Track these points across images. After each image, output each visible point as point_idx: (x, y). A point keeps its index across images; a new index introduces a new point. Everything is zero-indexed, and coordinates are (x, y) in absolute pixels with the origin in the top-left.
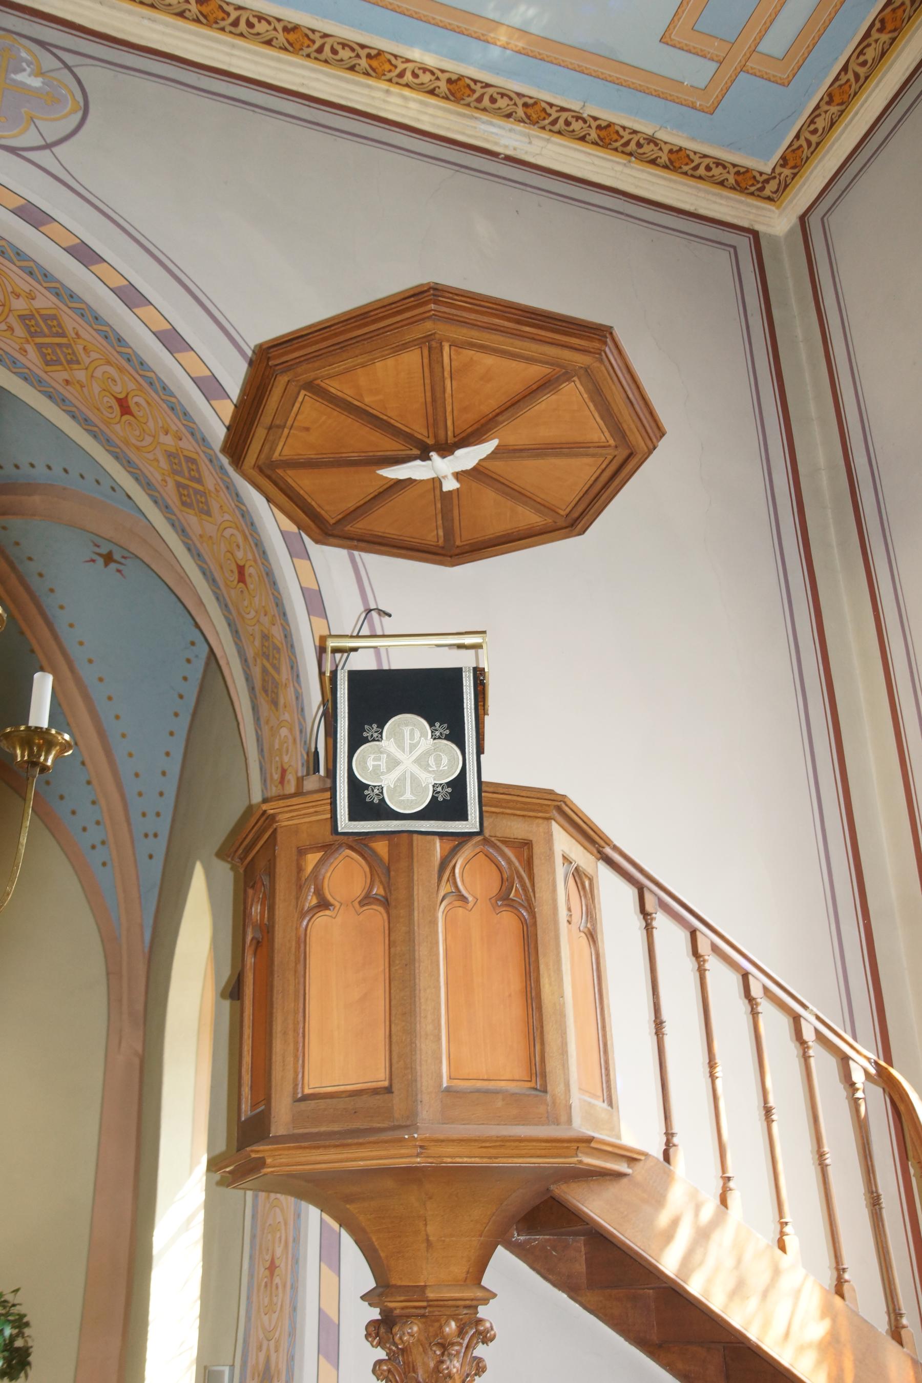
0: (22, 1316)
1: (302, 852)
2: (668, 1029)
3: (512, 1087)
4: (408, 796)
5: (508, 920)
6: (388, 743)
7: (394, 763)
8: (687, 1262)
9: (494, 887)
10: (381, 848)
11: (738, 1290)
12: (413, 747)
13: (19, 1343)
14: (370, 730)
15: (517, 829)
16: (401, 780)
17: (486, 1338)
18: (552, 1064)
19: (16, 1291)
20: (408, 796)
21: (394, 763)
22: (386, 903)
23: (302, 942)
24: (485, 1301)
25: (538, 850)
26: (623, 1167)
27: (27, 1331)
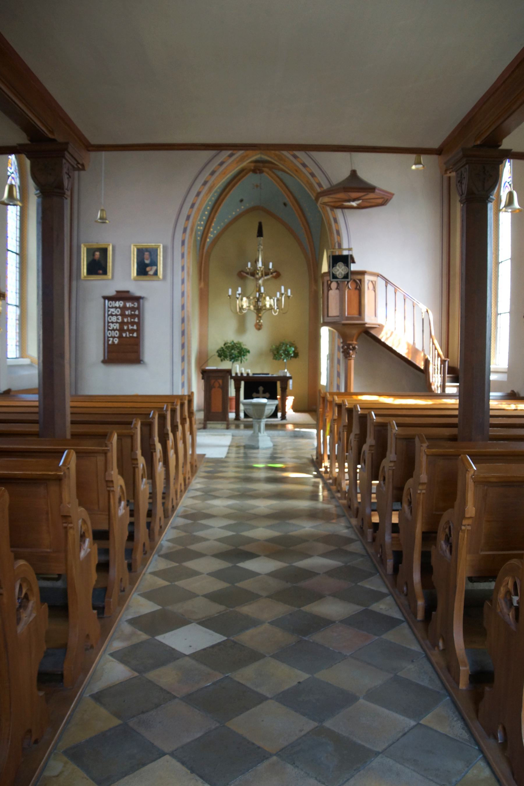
6: (338, 267)
8: (387, 339)
10: (339, 282)
12: (341, 267)
15: (359, 277)
16: (339, 273)
20: (340, 275)
25: (362, 280)
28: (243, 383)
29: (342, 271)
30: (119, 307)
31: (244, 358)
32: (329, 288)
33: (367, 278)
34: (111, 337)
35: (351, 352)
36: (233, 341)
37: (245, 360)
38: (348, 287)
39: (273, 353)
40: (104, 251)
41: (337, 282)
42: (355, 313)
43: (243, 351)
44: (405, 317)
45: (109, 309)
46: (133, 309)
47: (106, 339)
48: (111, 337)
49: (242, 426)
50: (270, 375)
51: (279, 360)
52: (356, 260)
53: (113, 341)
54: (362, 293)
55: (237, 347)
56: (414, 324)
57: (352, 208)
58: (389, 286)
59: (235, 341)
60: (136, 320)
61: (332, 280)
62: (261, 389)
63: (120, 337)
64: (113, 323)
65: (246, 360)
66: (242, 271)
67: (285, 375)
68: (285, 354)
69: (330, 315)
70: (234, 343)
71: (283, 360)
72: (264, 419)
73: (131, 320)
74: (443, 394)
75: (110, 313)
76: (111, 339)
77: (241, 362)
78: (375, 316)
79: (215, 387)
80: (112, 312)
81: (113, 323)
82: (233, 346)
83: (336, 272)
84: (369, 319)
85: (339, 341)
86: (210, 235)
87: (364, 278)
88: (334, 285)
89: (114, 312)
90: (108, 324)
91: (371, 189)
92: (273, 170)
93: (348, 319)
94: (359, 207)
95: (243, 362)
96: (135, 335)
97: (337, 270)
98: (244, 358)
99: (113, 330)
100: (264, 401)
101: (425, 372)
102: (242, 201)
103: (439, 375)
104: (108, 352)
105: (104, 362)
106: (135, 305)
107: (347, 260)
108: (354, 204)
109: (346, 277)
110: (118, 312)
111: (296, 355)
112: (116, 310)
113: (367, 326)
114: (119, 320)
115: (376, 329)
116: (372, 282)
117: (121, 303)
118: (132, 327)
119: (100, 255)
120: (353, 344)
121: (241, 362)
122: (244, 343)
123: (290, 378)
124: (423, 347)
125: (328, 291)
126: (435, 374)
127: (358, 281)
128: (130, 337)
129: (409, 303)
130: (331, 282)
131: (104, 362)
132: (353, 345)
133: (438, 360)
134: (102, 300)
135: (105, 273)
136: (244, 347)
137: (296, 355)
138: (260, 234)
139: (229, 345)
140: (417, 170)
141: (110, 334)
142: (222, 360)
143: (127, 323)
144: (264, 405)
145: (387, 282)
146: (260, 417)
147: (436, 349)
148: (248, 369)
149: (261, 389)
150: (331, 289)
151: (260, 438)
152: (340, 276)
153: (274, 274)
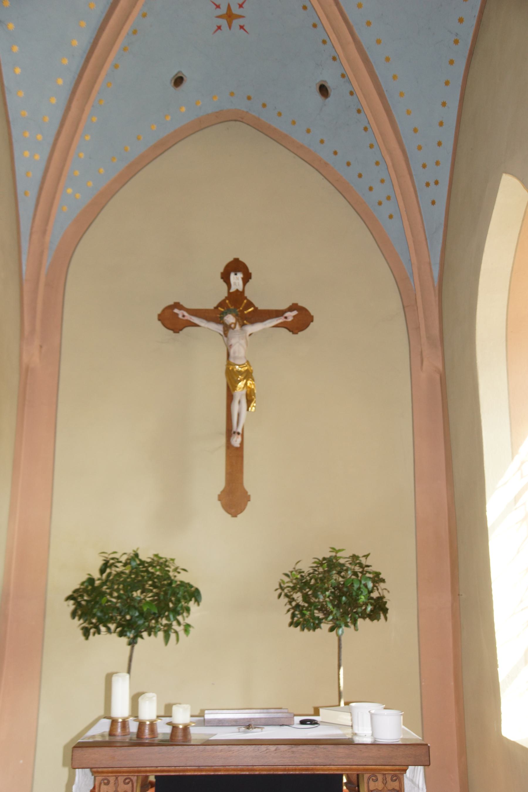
19: (366, 556)
27: (382, 585)
31: (179, 624)
36: (136, 555)
37: (180, 629)
39: (291, 600)
43: (174, 594)
55: (152, 576)
59: (145, 556)
65: (187, 628)
66: (177, 305)
68: (338, 606)
70: (142, 563)
77: (167, 638)
82: (135, 571)
95: (173, 636)
98: (179, 624)
102: (179, 81)
121: (167, 638)
122: (179, 563)
136: (182, 577)
139: (120, 568)
153: (290, 315)
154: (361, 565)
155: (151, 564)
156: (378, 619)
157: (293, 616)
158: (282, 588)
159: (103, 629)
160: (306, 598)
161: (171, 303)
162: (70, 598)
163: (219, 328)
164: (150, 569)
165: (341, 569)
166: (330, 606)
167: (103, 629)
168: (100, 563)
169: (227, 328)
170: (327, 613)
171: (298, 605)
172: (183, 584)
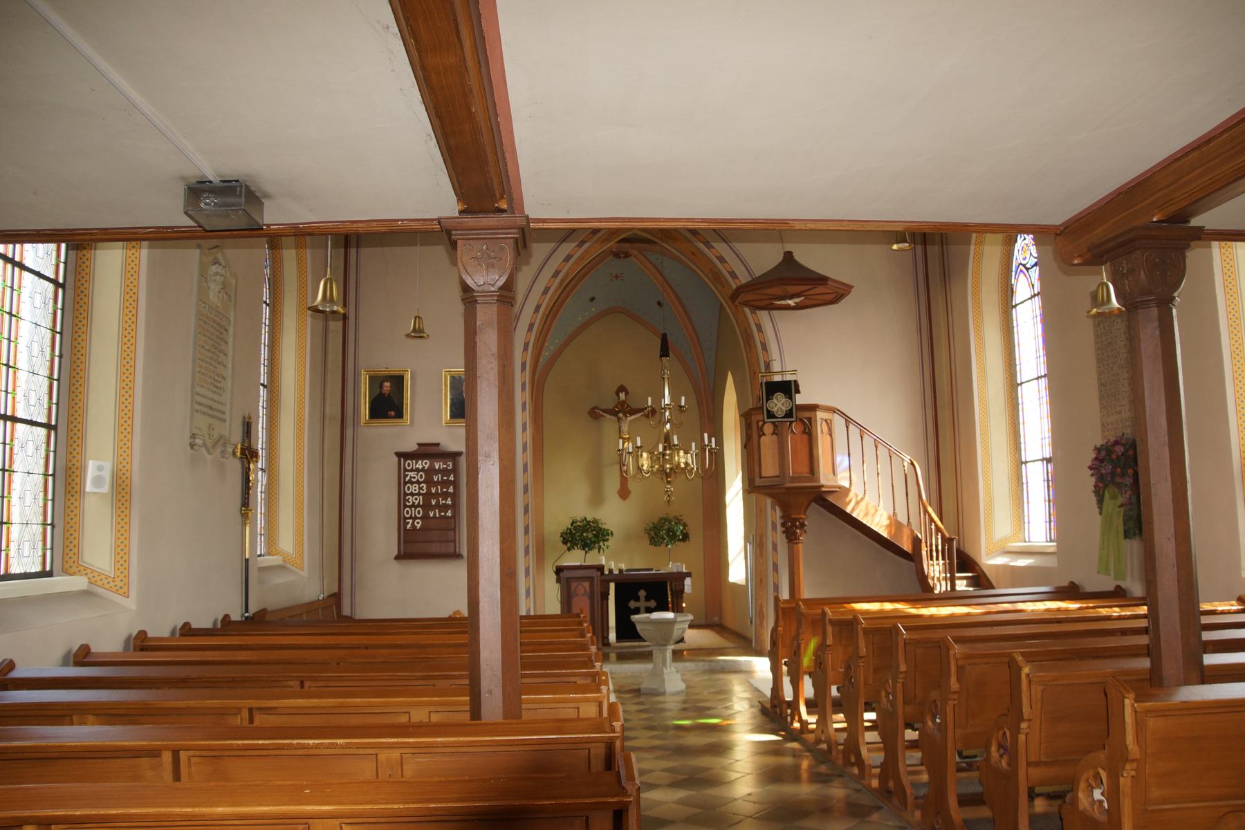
0: (685, 523)
1: (758, 422)
2: (851, 456)
3: (807, 475)
4: (780, 413)
5: (806, 436)
6: (775, 401)
7: (776, 405)
8: (853, 510)
9: (802, 428)
11: (866, 514)
13: (684, 531)
14: (770, 397)
15: (807, 414)
16: (778, 409)
17: (805, 525)
18: (816, 470)
20: (780, 413)
21: (776, 405)
22: (776, 434)
23: (759, 442)
24: (806, 518)
25: (813, 420)
26: (838, 490)
28: (612, 586)
29: (782, 407)
30: (423, 470)
31: (604, 545)
32: (761, 433)
33: (820, 415)
34: (410, 518)
35: (798, 531)
36: (585, 519)
37: (605, 548)
38: (792, 431)
39: (649, 535)
40: (398, 380)
41: (773, 423)
42: (804, 469)
44: (878, 474)
45: (407, 473)
46: (445, 472)
47: (402, 520)
48: (410, 518)
49: (613, 656)
50: (654, 572)
51: (660, 545)
52: (801, 389)
53: (413, 523)
54: (814, 440)
56: (892, 484)
57: (788, 308)
58: (851, 427)
60: (451, 490)
61: (766, 420)
62: (642, 593)
63: (425, 517)
64: (412, 495)
65: (608, 547)
66: (596, 407)
67: (680, 570)
68: (669, 536)
69: (763, 475)
71: (667, 545)
72: (670, 645)
73: (441, 490)
74: (954, 594)
75: (408, 479)
76: (411, 521)
77: (599, 551)
78: (834, 474)
79: (577, 595)
80: (411, 477)
81: (412, 495)
82: (585, 526)
83: (772, 408)
84: (825, 479)
85: (774, 515)
86: (543, 352)
87: (816, 416)
88: (768, 428)
89: (414, 478)
90: (405, 497)
91: (823, 280)
92: (645, 253)
93: (793, 479)
94: (798, 307)
95: (601, 550)
96: (449, 514)
97: (774, 405)
98: (604, 545)
99: (413, 506)
100: (670, 615)
101: (913, 557)
102: (592, 299)
103: (941, 562)
104: (405, 542)
105: (398, 558)
106: (448, 466)
107: (789, 388)
108: (791, 302)
109: (789, 414)
110: (421, 477)
111: (686, 537)
112: (417, 475)
113: (823, 489)
114: (423, 490)
115: (835, 494)
116: (826, 421)
117: (426, 463)
118: (444, 502)
119: (390, 387)
120: (801, 518)
121: (599, 551)
122: (603, 521)
123: (689, 575)
124: (909, 519)
125: (760, 437)
126: (932, 559)
127: (806, 421)
128: (441, 517)
129: (882, 451)
130: (765, 423)
131: (398, 558)
132: (801, 521)
133: (937, 539)
134: (396, 459)
135: (400, 415)
136: (604, 527)
137: (686, 537)
138: (665, 352)
139: (579, 524)
140: (899, 250)
141: (408, 512)
142: (569, 549)
143: (437, 495)
144: (671, 623)
145: (848, 420)
146: (664, 643)
147: (932, 520)
148: (621, 563)
149: (642, 593)
150: (764, 434)
151: (666, 677)
152: (780, 414)
154: (677, 519)
155: (590, 522)
156: (686, 541)
157: (651, 541)
158: (646, 530)
159: (576, 548)
160: (655, 534)
161: (593, 406)
162: (561, 536)
163: (615, 419)
164: (591, 524)
165: (670, 521)
166: (665, 537)
167: (576, 548)
168: (571, 521)
169: (619, 419)
170: (664, 539)
171: (653, 537)
172: (604, 529)
